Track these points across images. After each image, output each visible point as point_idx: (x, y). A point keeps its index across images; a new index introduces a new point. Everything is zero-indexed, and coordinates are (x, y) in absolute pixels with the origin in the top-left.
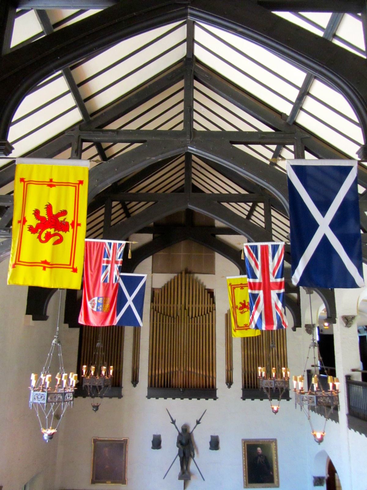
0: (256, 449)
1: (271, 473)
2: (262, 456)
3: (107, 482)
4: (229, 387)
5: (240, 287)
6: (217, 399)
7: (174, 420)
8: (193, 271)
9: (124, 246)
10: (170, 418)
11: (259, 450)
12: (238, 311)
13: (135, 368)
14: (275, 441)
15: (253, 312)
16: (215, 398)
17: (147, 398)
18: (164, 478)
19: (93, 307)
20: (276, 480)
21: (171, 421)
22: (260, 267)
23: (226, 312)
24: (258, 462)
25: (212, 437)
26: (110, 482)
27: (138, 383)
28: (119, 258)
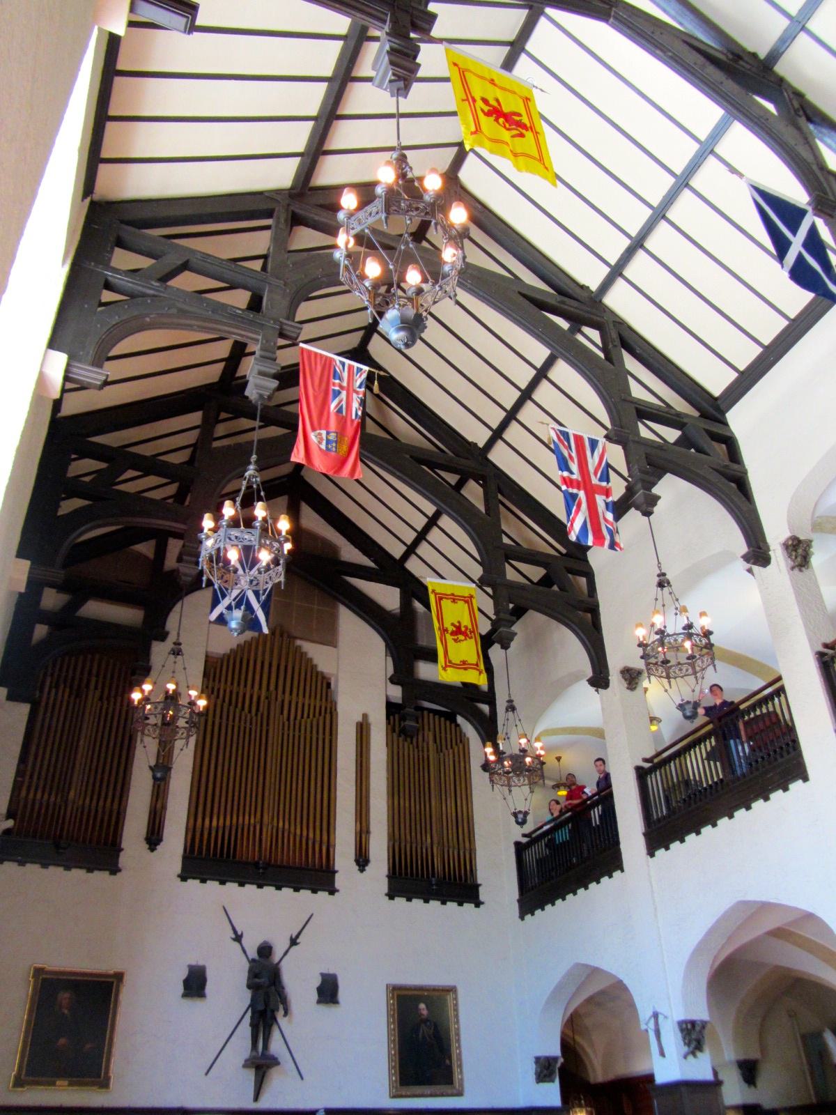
0: (417, 1008)
3: (58, 1083)
4: (362, 870)
5: (451, 598)
7: (239, 933)
8: (295, 635)
9: (366, 373)
10: (230, 927)
11: (423, 1009)
12: (449, 637)
13: (159, 806)
14: (452, 990)
15: (571, 518)
16: (333, 891)
17: (179, 879)
19: (320, 443)
20: (456, 1076)
21: (233, 936)
22: (576, 460)
23: (360, 719)
24: (420, 1036)
25: (323, 975)
26: (66, 1083)
27: (162, 844)
28: (360, 387)
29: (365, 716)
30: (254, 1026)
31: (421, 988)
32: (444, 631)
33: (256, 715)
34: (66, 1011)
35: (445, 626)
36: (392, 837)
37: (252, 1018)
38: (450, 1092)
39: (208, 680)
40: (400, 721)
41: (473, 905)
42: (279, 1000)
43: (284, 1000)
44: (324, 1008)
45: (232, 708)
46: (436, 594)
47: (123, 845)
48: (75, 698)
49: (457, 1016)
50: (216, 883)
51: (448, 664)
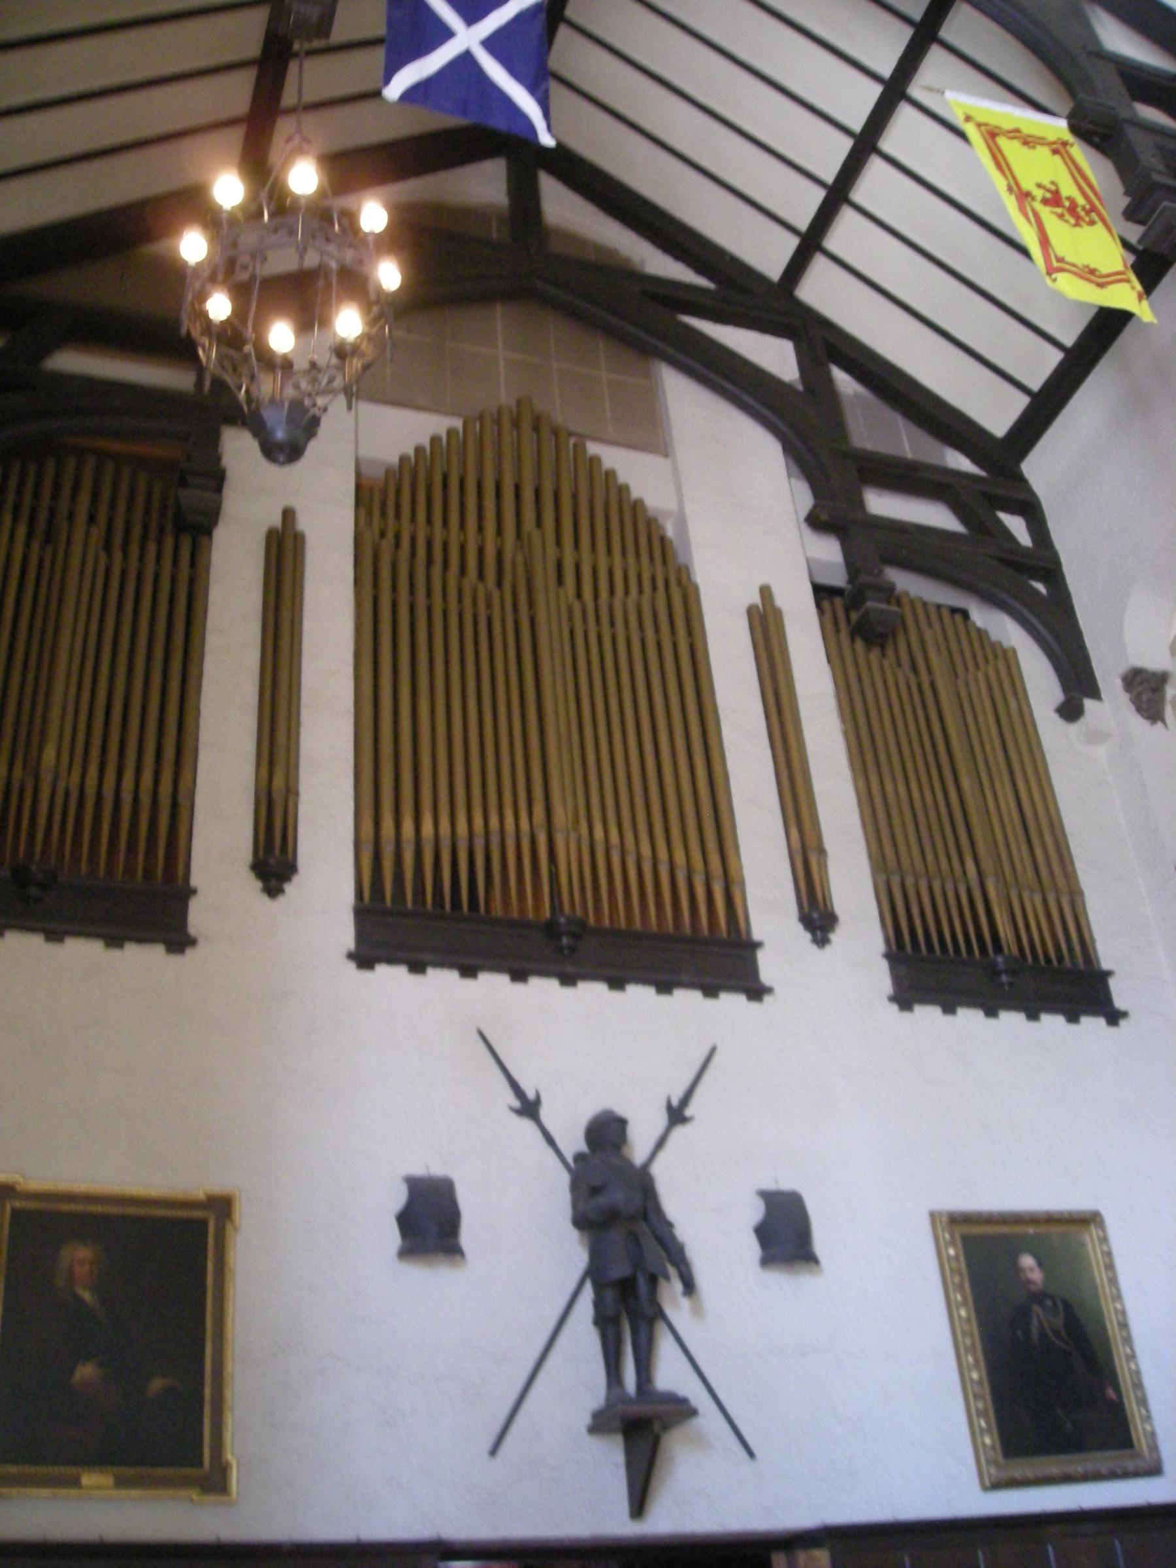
0: (1016, 1269)
1: (1111, 1393)
2: (1049, 1303)
7: (531, 1095)
11: (1031, 1269)
13: (278, 782)
14: (1090, 1220)
18: (493, 1452)
21: (516, 1104)
27: (296, 879)
29: (765, 592)
30: (605, 1322)
31: (1017, 1219)
33: (499, 584)
34: (86, 1296)
36: (879, 864)
37: (598, 1304)
38: (1130, 1465)
39: (370, 514)
40: (847, 611)
41: (1102, 1021)
42: (664, 1255)
43: (677, 1256)
44: (779, 1281)
45: (437, 570)
46: (979, 125)
47: (195, 881)
48: (43, 549)
49: (1114, 1281)
51: (1055, 264)
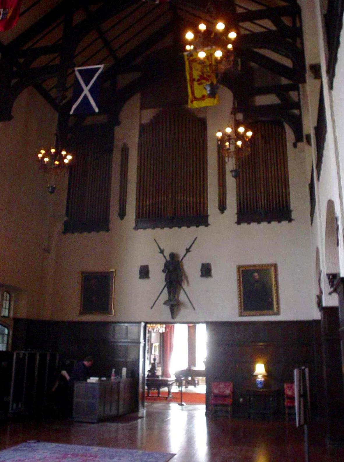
0: (253, 276)
6: (209, 226)
11: (257, 276)
12: (196, 83)
21: (159, 251)
24: (255, 288)
32: (192, 80)
35: (194, 77)
44: (204, 279)
50: (276, 223)
